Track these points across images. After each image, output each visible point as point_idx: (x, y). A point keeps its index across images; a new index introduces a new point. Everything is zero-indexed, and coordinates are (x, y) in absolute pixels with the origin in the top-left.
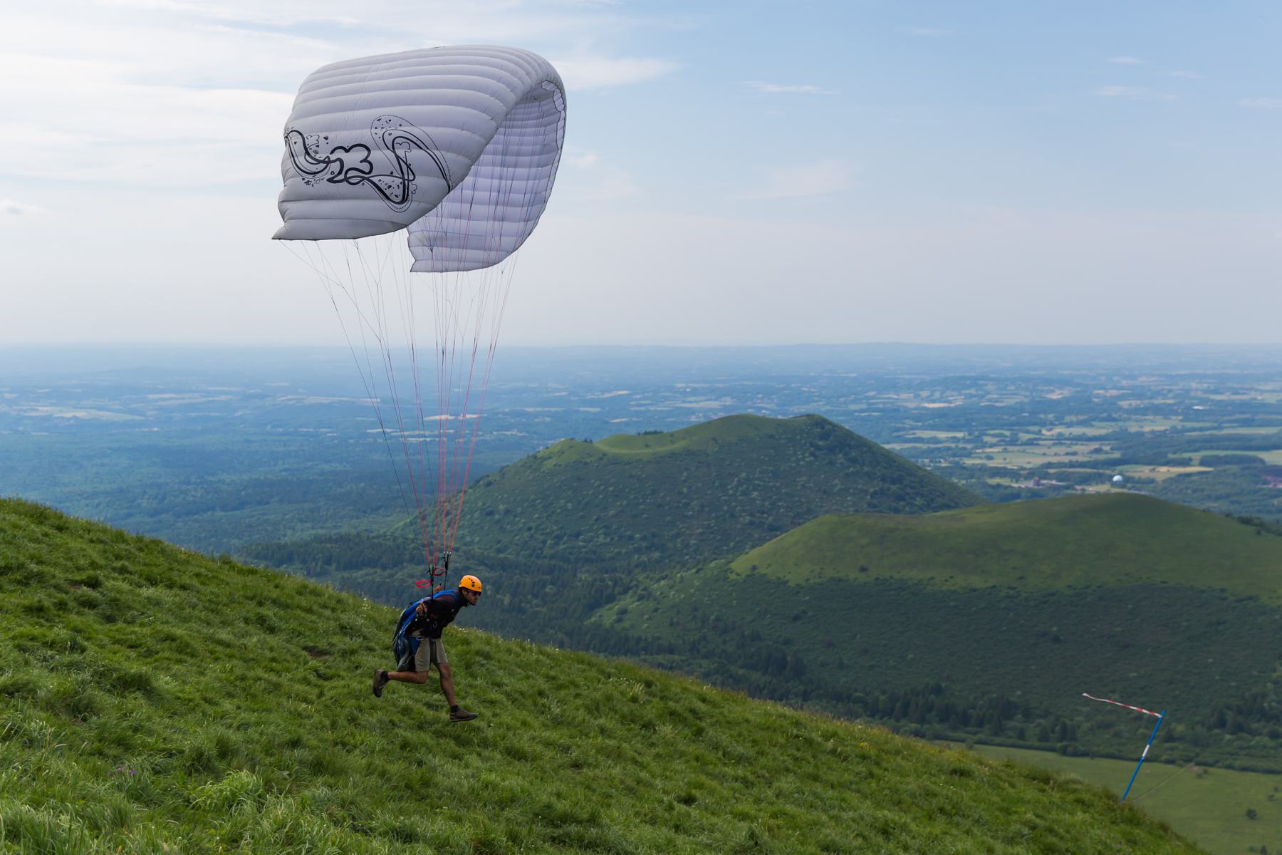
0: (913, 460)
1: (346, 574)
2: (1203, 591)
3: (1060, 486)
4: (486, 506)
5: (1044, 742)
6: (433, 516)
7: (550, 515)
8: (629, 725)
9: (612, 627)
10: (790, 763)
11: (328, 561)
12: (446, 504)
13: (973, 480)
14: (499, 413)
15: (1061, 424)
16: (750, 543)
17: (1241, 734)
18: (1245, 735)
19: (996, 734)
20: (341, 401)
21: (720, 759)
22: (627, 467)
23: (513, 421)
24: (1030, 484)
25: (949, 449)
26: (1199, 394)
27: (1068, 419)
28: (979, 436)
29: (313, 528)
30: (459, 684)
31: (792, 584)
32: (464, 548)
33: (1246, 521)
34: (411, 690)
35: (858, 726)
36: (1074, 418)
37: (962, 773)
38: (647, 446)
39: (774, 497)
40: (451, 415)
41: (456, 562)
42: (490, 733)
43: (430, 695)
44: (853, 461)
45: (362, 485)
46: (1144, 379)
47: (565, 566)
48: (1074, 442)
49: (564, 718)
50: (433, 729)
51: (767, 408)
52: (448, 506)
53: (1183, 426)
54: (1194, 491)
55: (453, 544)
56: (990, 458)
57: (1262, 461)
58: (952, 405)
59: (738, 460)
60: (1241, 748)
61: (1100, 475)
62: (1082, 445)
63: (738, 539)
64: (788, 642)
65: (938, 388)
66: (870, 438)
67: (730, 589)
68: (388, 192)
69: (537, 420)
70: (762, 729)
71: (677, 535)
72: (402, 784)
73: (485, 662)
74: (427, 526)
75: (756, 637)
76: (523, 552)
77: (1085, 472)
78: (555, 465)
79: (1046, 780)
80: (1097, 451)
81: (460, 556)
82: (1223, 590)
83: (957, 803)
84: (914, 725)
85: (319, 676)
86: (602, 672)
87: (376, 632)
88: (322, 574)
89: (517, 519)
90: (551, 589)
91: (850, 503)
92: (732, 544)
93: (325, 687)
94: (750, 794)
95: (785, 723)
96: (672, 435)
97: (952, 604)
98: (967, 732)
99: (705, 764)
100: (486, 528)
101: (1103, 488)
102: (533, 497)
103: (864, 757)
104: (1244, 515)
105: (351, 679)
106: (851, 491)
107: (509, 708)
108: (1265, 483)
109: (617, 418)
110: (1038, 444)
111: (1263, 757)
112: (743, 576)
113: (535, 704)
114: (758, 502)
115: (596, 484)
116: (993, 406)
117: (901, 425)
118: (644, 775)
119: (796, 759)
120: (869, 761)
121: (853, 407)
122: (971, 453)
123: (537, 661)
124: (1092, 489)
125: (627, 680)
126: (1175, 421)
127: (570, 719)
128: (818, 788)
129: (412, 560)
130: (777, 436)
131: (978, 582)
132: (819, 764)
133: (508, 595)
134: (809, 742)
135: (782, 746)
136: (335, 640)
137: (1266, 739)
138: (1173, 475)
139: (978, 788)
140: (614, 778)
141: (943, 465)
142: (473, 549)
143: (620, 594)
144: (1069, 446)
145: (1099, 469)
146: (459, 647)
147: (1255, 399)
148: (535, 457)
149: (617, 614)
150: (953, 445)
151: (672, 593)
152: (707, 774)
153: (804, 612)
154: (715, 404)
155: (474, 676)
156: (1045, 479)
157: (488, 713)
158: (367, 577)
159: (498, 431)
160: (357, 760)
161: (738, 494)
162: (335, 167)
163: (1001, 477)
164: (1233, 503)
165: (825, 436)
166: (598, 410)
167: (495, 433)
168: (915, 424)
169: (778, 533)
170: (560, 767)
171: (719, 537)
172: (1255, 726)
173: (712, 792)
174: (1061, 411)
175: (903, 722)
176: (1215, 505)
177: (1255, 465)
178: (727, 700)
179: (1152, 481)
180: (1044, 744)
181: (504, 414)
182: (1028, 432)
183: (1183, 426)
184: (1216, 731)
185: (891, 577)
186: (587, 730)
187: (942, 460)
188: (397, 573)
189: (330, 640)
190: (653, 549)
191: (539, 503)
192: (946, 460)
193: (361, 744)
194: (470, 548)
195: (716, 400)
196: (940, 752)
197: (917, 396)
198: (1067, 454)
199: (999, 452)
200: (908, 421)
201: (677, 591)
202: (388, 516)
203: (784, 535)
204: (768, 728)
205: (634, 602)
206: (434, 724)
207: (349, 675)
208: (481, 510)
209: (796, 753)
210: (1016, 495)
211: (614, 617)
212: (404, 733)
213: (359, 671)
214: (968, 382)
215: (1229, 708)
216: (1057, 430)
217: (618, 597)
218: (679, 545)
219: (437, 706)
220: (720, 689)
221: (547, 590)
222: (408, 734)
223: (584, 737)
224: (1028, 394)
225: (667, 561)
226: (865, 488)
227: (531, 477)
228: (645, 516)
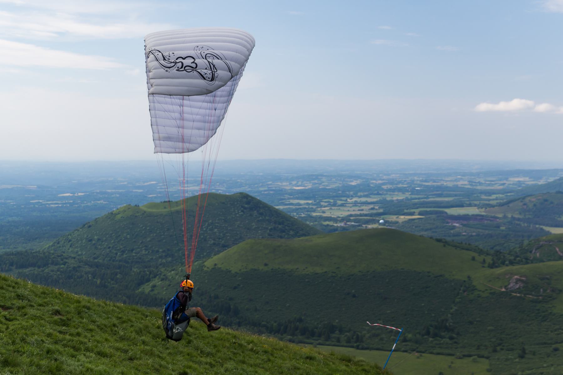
0: (289, 214)
1: (20, 271)
2: (420, 273)
3: (356, 225)
4: (88, 237)
5: (349, 343)
6: (62, 242)
7: (119, 241)
8: (156, 339)
9: (149, 293)
10: (231, 355)
11: (12, 264)
12: (69, 236)
13: (316, 223)
14: (94, 193)
15: (356, 196)
16: (214, 253)
19: (327, 340)
20: (17, 187)
21: (199, 354)
22: (156, 218)
23: (101, 196)
24: (342, 224)
25: (305, 208)
26: (418, 182)
27: (359, 194)
28: (319, 202)
29: (4, 249)
30: (74, 322)
31: (233, 272)
32: (78, 257)
33: (439, 241)
34: (52, 325)
35: (263, 337)
36: (362, 194)
37: (310, 358)
38: (165, 208)
39: (225, 231)
40: (71, 194)
41: (74, 264)
42: (90, 345)
43: (61, 327)
44: (261, 214)
45: (28, 227)
46: (394, 175)
47: (127, 265)
48: (362, 205)
49: (125, 337)
50: (62, 343)
51: (221, 190)
52: (70, 237)
53: (411, 197)
54: (416, 227)
55: (73, 255)
56: (324, 212)
57: (446, 213)
58: (307, 188)
59: (208, 214)
61: (374, 220)
62: (366, 206)
63: (208, 251)
64: (231, 299)
65: (300, 180)
66: (269, 203)
67: (204, 275)
68: (205, 76)
69: (113, 196)
70: (219, 340)
71: (179, 250)
72: (47, 370)
73: (87, 311)
74: (60, 247)
75: (216, 297)
76: (106, 259)
77: (367, 219)
78: (121, 217)
79: (349, 361)
80: (372, 209)
81: (76, 261)
82: (429, 272)
83: (308, 372)
84: (289, 337)
85: (6, 319)
86: (144, 315)
87: (34, 298)
88: (9, 270)
89: (103, 243)
90: (119, 276)
91: (260, 234)
92: (205, 254)
93: (10, 324)
94: (213, 371)
95: (229, 337)
96: (177, 202)
97: (307, 280)
98: (314, 340)
99: (192, 357)
100: (89, 247)
101: (375, 226)
102: (111, 232)
103: (266, 352)
104: (438, 238)
105: (22, 320)
106: (260, 228)
107: (99, 332)
108: (448, 223)
109: (151, 194)
110: (346, 206)
112: (210, 268)
113: (112, 331)
114: (217, 234)
115: (141, 226)
116: (326, 188)
117: (283, 197)
118: (163, 363)
119: (234, 354)
120: (268, 353)
121: (261, 189)
122: (315, 210)
123: (113, 310)
124: (370, 226)
125: (155, 318)
126: (408, 195)
127: (128, 337)
128: (245, 366)
129: (52, 264)
130: (226, 203)
131: (318, 270)
132: (245, 355)
133: (99, 279)
134: (241, 345)
135: (228, 348)
136: (15, 302)
138: (406, 220)
139: (318, 365)
140: (149, 364)
141: (303, 215)
142: (82, 258)
143: (152, 278)
144: (360, 207)
145: (373, 217)
146: (75, 304)
147: (443, 184)
148: (112, 213)
149: (151, 287)
150: (307, 207)
151: (177, 277)
152: (193, 362)
153: (239, 285)
154: (197, 188)
155: (82, 318)
156: (348, 222)
157: (89, 335)
158: (31, 272)
159: (94, 201)
160: (25, 359)
161: (208, 230)
162: (179, 65)
163: (329, 221)
165: (248, 203)
166: (141, 191)
167: (92, 202)
168: (289, 197)
169: (227, 248)
170: (123, 360)
171: (199, 251)
172: (443, 334)
173: (195, 370)
174: (356, 191)
175: (284, 335)
176: (425, 233)
177: (443, 215)
178: (202, 326)
179: (397, 222)
180: (348, 344)
181: (97, 193)
182: (341, 200)
183: (411, 197)
185: (279, 268)
186: (136, 342)
187: (302, 214)
188: (45, 270)
189: (12, 302)
190: (168, 256)
191: (114, 235)
192: (304, 213)
193: (27, 351)
194: (81, 257)
195: (197, 186)
196: (301, 349)
197: (291, 184)
198: (359, 210)
199: (328, 210)
200: (286, 195)
201: (179, 276)
202: (41, 242)
203: (230, 249)
204: (222, 339)
205: (159, 282)
206: (63, 341)
207: (22, 318)
208: (86, 239)
209: (234, 351)
210: (336, 229)
211: (150, 289)
212: (48, 346)
213: (26, 317)
214: (314, 177)
215: (431, 326)
216: (354, 199)
217: (151, 279)
218: (180, 255)
219: (64, 333)
220: (199, 321)
221: (118, 277)
222: (51, 346)
223: (135, 346)
224: (341, 182)
225: (175, 262)
226: (267, 227)
227: (110, 223)
228: (164, 241)
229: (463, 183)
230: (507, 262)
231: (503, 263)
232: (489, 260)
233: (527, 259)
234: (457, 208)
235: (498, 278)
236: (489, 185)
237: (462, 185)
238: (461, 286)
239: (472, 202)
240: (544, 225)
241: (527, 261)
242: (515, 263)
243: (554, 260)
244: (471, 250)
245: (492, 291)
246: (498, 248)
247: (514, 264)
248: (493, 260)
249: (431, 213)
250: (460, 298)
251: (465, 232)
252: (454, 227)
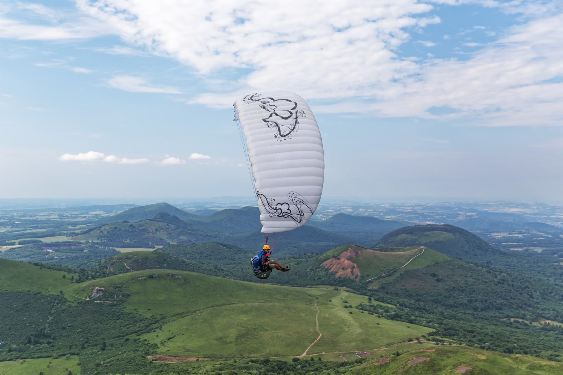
2: (21, 293)
17: (37, 344)
18: (38, 345)
26: (17, 217)
33: (36, 264)
57: (41, 242)
60: (37, 350)
82: (29, 291)
104: (35, 262)
111: (45, 352)
126: (9, 228)
137: (46, 345)
138: (9, 249)
147: (38, 219)
164: (31, 258)
172: (42, 341)
177: (39, 243)
184: (28, 345)
215: (32, 335)
229: (54, 217)
230: (90, 277)
231: (87, 278)
232: (76, 276)
233: (104, 273)
234: (50, 237)
235: (83, 290)
236: (74, 218)
237: (53, 218)
238: (56, 300)
239: (61, 232)
241: (104, 275)
242: (96, 277)
243: (124, 273)
244: (62, 270)
245: (80, 301)
246: (82, 267)
247: (95, 278)
248: (79, 276)
249: (29, 242)
250: (55, 310)
251: (57, 256)
252: (48, 253)
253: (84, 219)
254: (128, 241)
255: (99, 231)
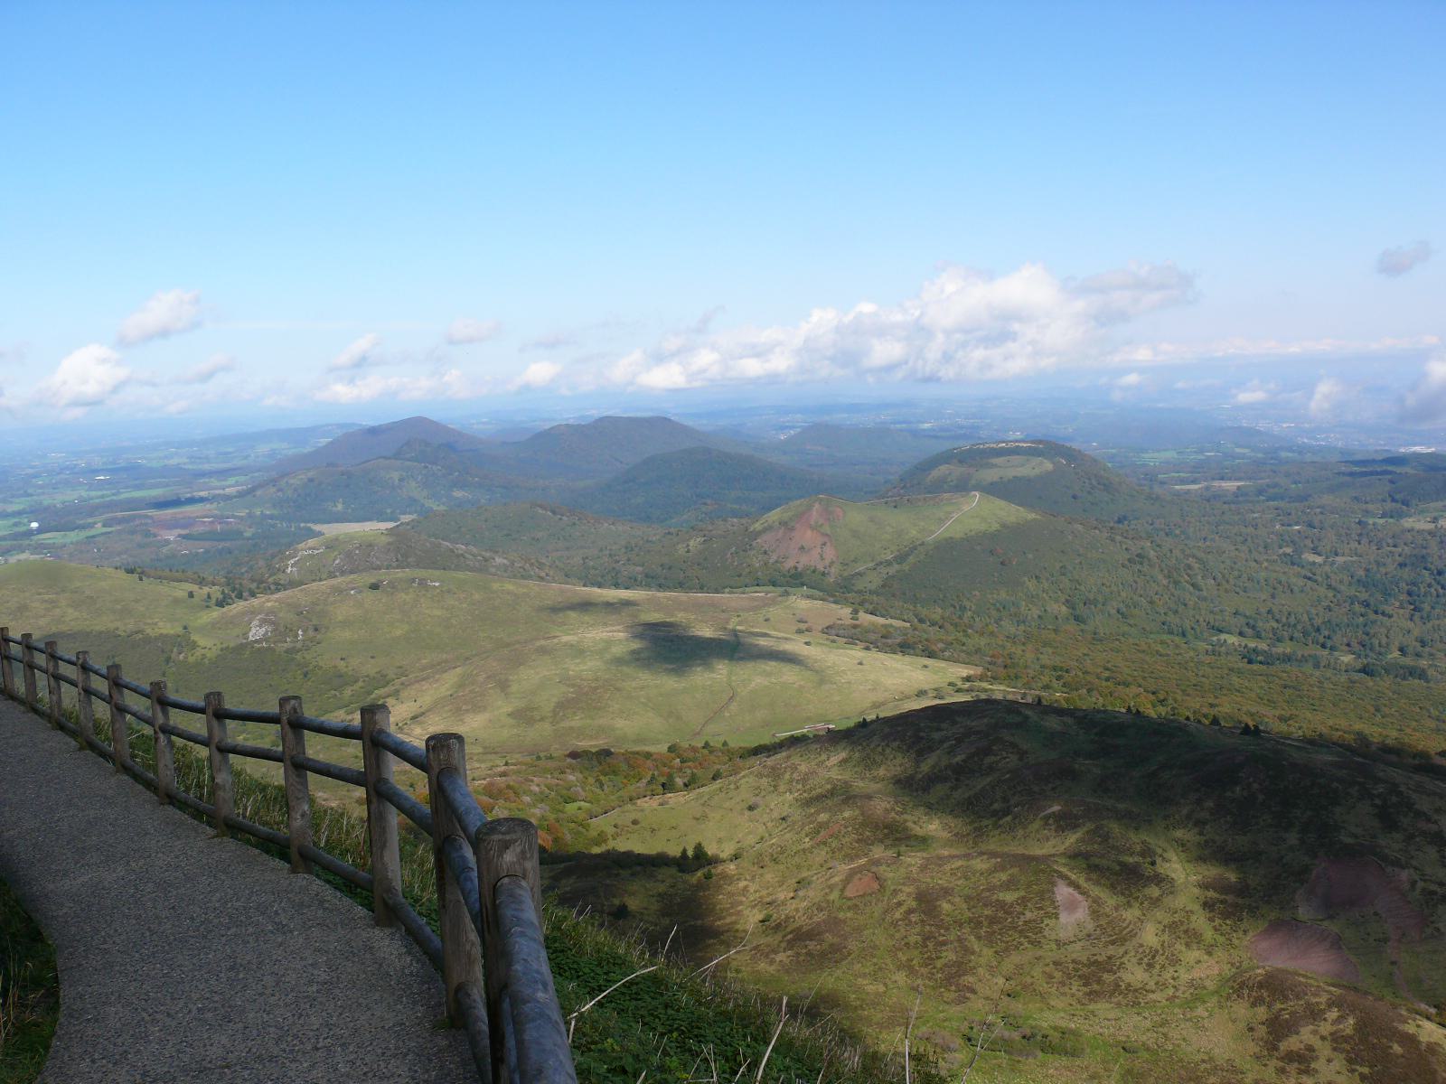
80: (16, 525)
240: (314, 522)
245: (224, 646)
252: (167, 542)
253: (245, 462)
254: (340, 507)
255: (274, 489)
